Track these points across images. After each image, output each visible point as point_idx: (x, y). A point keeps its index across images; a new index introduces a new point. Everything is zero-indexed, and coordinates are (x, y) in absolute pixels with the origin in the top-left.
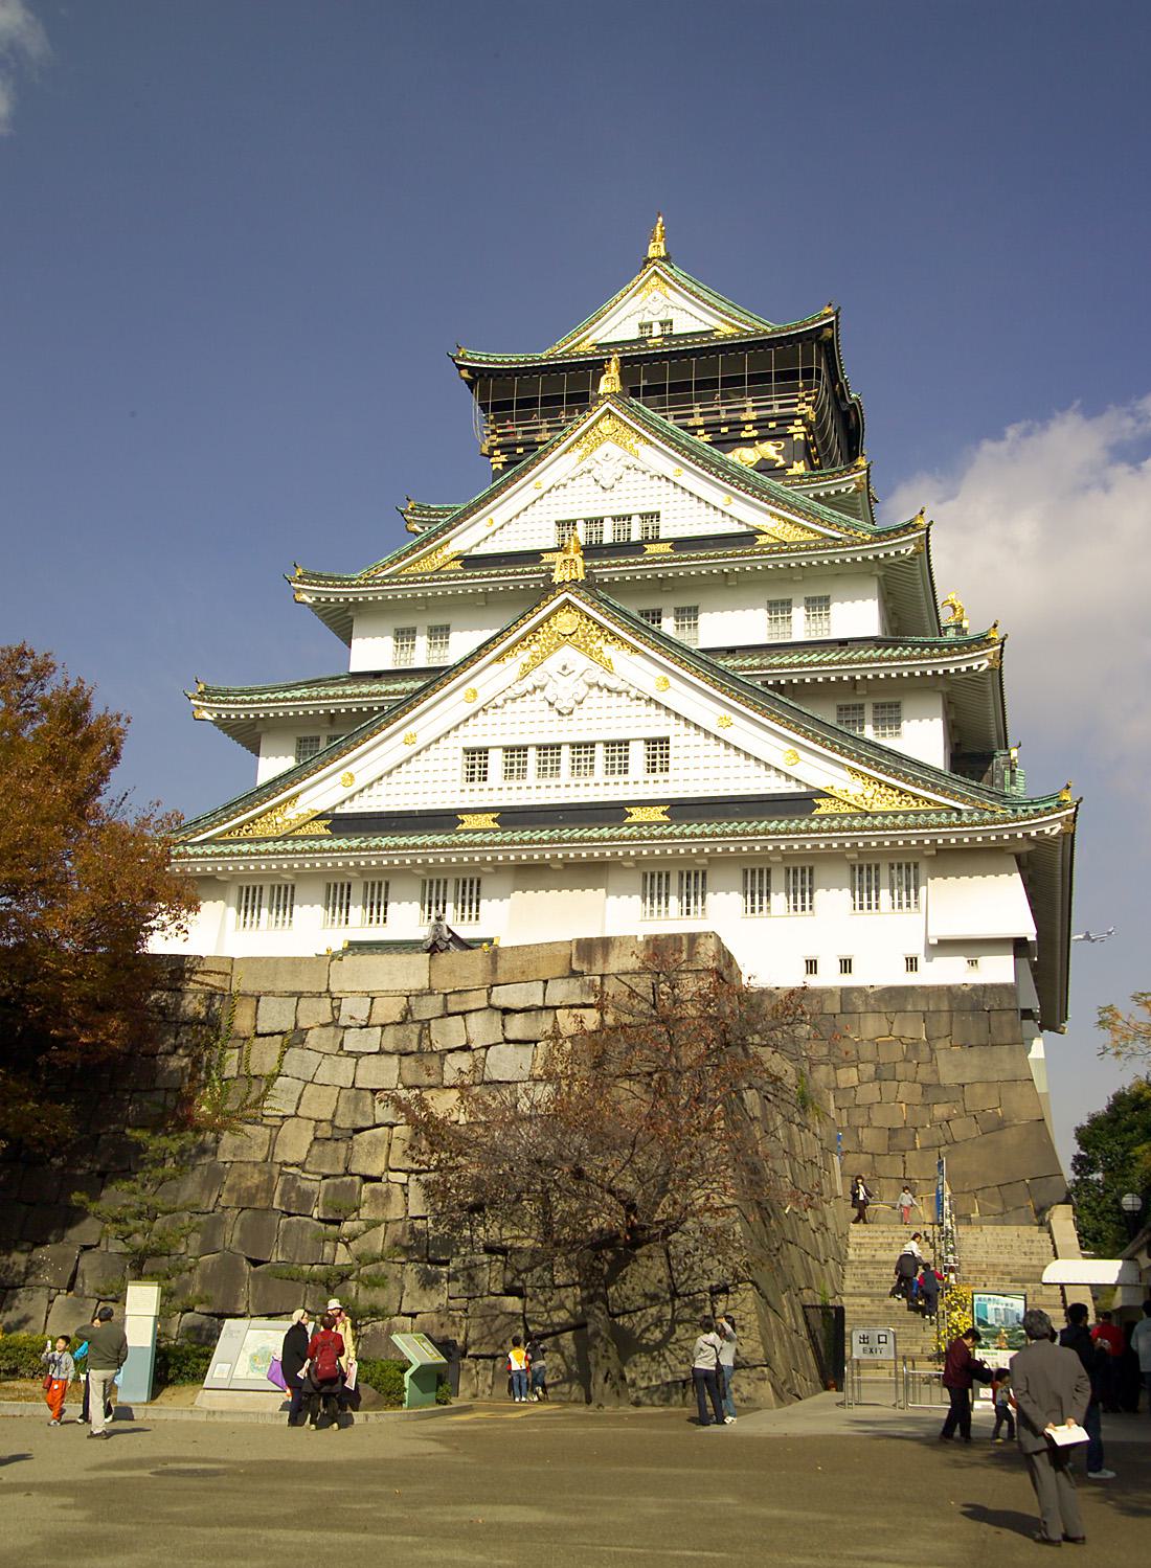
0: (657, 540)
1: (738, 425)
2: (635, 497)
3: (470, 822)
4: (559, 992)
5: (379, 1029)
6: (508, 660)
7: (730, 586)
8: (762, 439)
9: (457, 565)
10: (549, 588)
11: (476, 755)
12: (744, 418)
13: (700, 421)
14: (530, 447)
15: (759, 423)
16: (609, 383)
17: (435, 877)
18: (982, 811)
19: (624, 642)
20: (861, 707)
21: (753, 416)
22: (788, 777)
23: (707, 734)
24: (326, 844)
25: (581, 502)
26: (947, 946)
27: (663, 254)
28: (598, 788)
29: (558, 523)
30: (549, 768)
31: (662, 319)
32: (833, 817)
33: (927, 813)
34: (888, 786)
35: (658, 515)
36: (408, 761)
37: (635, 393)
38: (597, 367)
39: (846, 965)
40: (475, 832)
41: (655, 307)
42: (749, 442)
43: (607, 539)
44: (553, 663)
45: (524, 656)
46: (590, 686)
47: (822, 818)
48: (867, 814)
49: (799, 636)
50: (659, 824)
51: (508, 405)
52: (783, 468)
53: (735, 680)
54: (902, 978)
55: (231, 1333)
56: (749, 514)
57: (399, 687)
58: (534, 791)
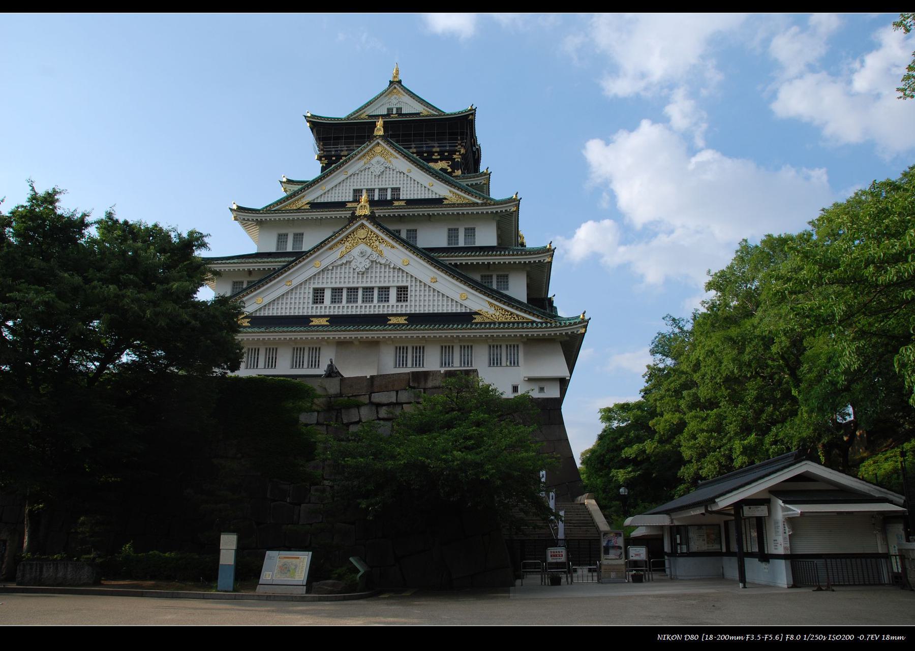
0: (399, 200)
2: (389, 183)
3: (316, 322)
4: (404, 396)
5: (316, 414)
6: (335, 249)
8: (441, 160)
9: (308, 207)
12: (434, 150)
13: (415, 150)
14: (339, 157)
16: (379, 131)
17: (299, 346)
18: (546, 323)
19: (388, 244)
20: (491, 276)
21: (438, 149)
22: (461, 305)
23: (425, 285)
24: (249, 330)
25: (365, 182)
26: (531, 380)
27: (397, 80)
28: (375, 308)
29: (354, 190)
30: (352, 298)
31: (398, 106)
32: (481, 323)
33: (523, 323)
34: (506, 311)
35: (399, 189)
36: (287, 293)
37: (392, 136)
38: (374, 125)
40: (318, 326)
41: (395, 101)
42: (436, 161)
43: (376, 198)
44: (356, 252)
46: (372, 262)
47: (477, 324)
48: (494, 323)
49: (461, 244)
50: (403, 325)
51: (329, 139)
52: (450, 174)
53: (437, 262)
55: (270, 558)
56: (441, 190)
57: (283, 259)
58: (345, 308)
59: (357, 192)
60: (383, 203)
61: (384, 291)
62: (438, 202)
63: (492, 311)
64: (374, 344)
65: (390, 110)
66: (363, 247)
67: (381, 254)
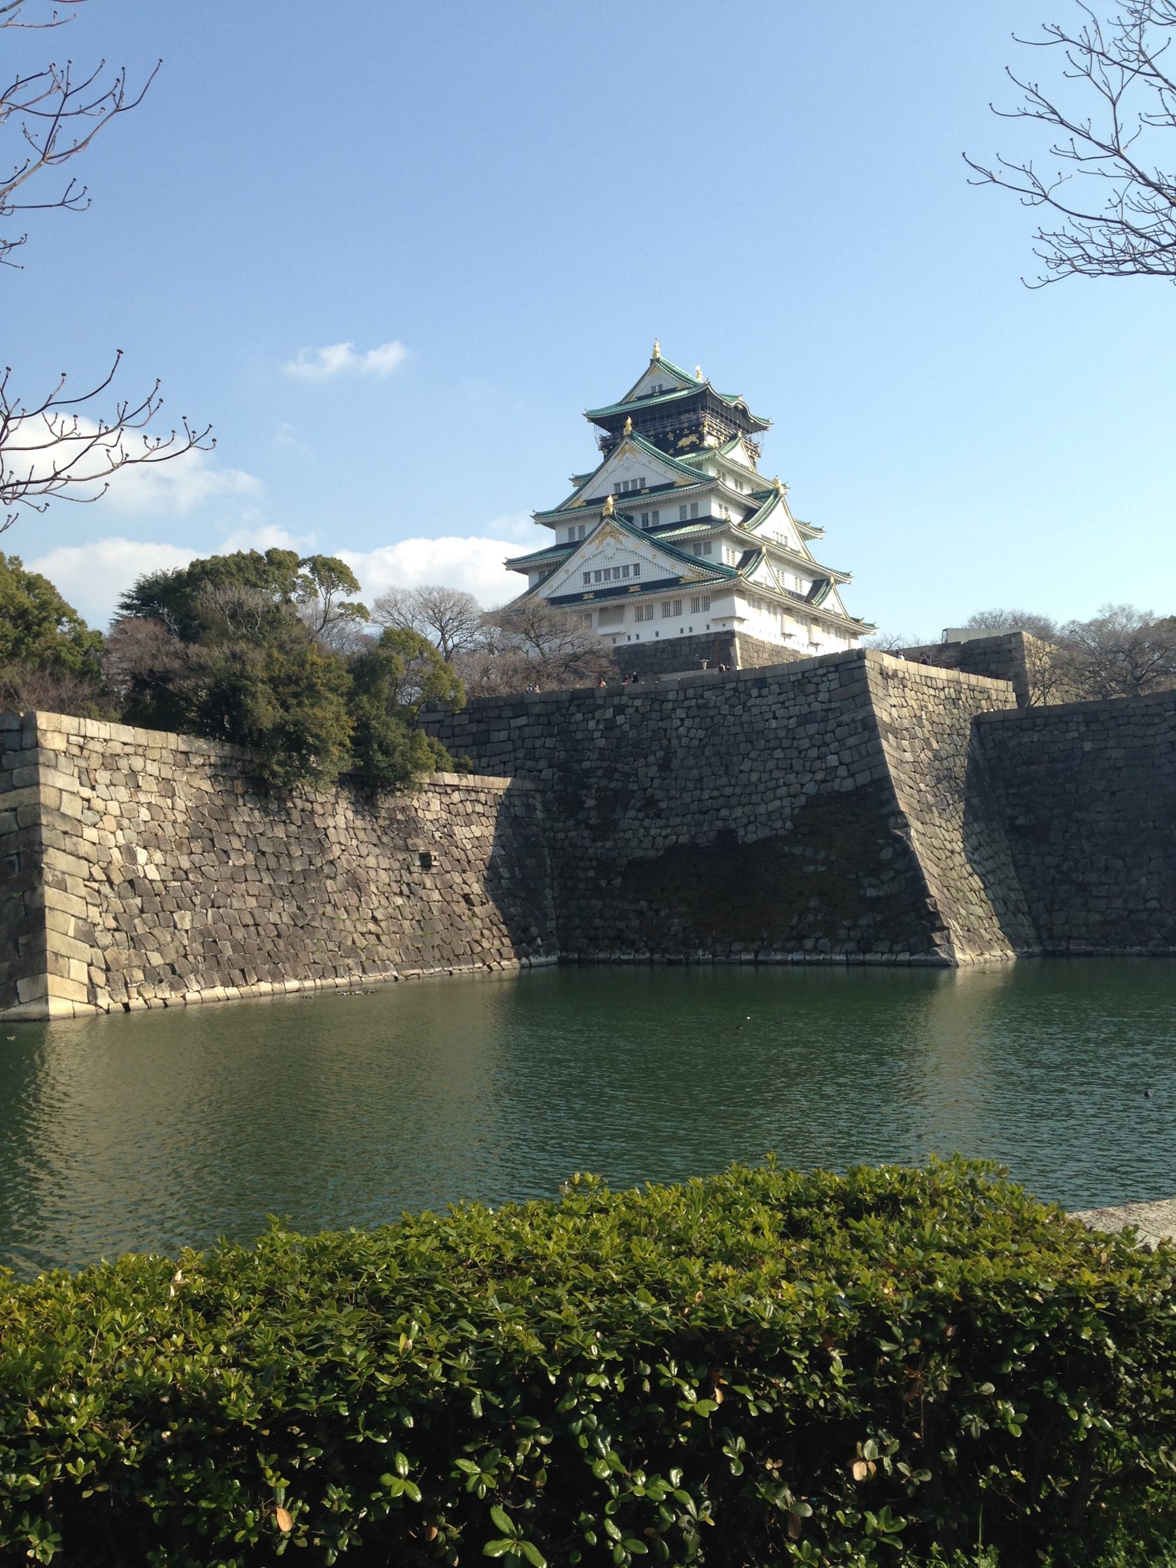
1: (682, 430)
7: (669, 501)
8: (691, 433)
10: (602, 518)
11: (587, 575)
13: (668, 429)
15: (689, 428)
21: (686, 425)
39: (691, 629)
42: (687, 436)
44: (605, 543)
45: (597, 541)
49: (689, 518)
54: (704, 631)
56: (672, 476)
59: (617, 485)
60: (636, 493)
61: (626, 568)
62: (670, 486)
63: (690, 574)
64: (622, 607)
65: (654, 388)
66: (609, 539)
67: (621, 543)
